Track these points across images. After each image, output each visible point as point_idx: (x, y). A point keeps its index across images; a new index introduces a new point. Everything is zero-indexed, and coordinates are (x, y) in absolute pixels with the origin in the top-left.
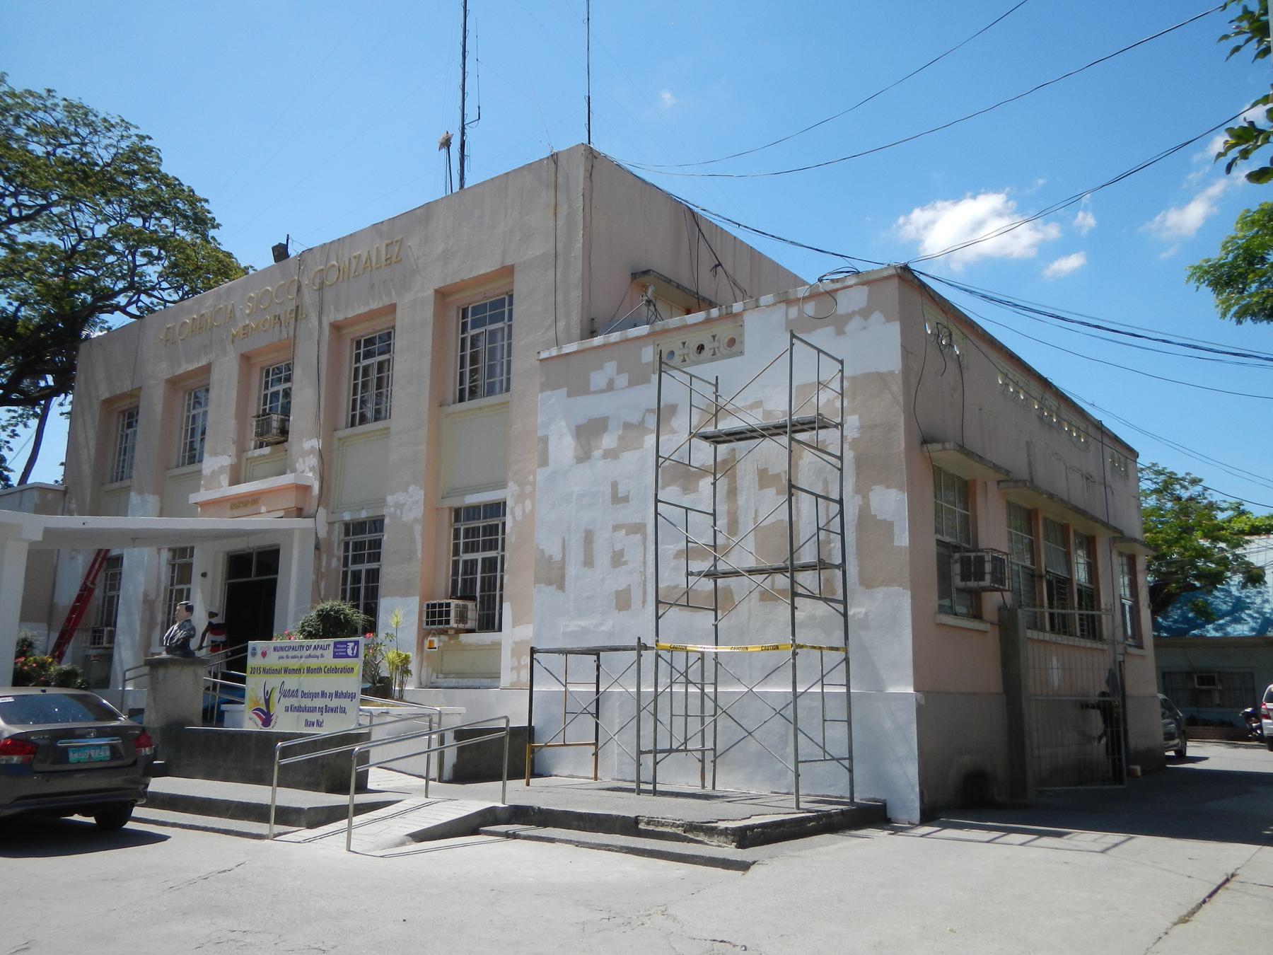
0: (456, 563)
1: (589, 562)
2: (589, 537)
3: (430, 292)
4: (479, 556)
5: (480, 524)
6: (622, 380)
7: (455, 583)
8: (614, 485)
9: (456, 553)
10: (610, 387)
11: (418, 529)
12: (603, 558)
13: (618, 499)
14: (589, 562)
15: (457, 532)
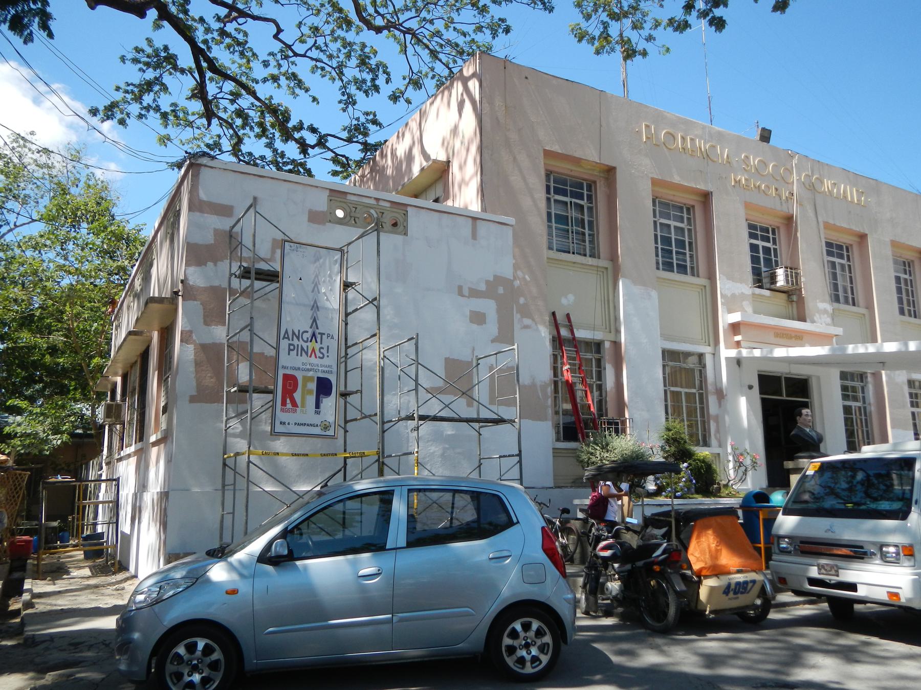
3: (887, 239)
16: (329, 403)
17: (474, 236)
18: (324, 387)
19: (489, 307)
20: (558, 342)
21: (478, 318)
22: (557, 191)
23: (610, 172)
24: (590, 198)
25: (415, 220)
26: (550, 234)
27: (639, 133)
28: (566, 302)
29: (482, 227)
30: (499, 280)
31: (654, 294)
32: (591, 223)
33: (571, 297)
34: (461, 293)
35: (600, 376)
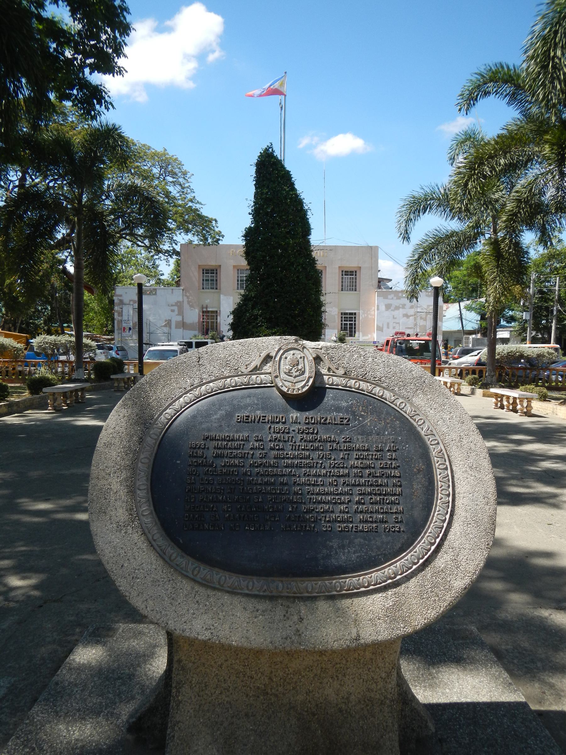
0: (342, 324)
1: (388, 328)
2: (388, 324)
3: (337, 267)
4: (348, 323)
5: (348, 316)
6: (395, 298)
7: (342, 328)
8: (394, 316)
9: (342, 321)
10: (392, 299)
11: (336, 317)
12: (391, 327)
13: (394, 318)
14: (388, 328)
15: (342, 318)
16: (131, 331)
17: (172, 293)
18: (130, 329)
19: (176, 308)
20: (203, 312)
21: (173, 311)
22: (206, 273)
23: (220, 266)
24: (216, 273)
25: (158, 292)
26: (203, 284)
27: (230, 254)
28: (207, 301)
29: (174, 291)
30: (178, 302)
31: (232, 298)
32: (216, 280)
33: (208, 300)
34: (169, 306)
35: (217, 319)
